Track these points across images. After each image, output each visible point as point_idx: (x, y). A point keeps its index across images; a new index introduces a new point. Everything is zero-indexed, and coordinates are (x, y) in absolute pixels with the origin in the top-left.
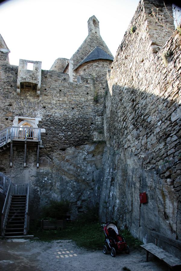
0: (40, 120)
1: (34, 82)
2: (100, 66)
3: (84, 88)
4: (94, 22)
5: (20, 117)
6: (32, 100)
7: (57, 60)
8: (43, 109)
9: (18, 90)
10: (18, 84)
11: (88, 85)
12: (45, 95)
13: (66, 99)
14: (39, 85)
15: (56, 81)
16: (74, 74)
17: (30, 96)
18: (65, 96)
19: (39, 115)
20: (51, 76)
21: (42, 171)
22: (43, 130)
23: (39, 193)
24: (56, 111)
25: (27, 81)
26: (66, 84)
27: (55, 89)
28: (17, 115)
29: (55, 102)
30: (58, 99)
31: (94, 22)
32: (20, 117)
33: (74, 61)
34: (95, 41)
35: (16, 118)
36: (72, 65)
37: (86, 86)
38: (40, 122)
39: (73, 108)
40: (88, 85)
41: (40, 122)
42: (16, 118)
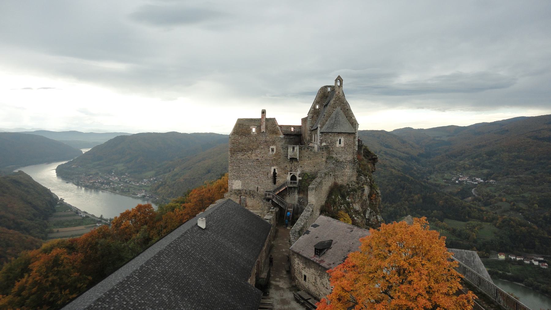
0: (299, 173)
1: (296, 157)
2: (332, 135)
3: (321, 154)
4: (339, 79)
5: (291, 172)
6: (296, 163)
7: (320, 90)
8: (300, 168)
9: (290, 160)
10: (289, 158)
11: (323, 152)
12: (302, 160)
13: (311, 161)
14: (298, 158)
15: (306, 152)
16: (321, 134)
17: (295, 161)
18: (311, 160)
19: (298, 171)
20: (304, 149)
21: (300, 197)
22: (301, 178)
23: (298, 206)
24: (307, 168)
25: (292, 157)
26: (312, 153)
27: (306, 157)
28: (289, 171)
29: (306, 164)
30: (307, 162)
31: (339, 79)
32: (291, 172)
33: (321, 124)
34: (337, 102)
35: (289, 173)
36: (320, 128)
37: (322, 152)
38: (299, 174)
39: (315, 166)
40: (323, 152)
41: (299, 174)
42: (289, 173)
